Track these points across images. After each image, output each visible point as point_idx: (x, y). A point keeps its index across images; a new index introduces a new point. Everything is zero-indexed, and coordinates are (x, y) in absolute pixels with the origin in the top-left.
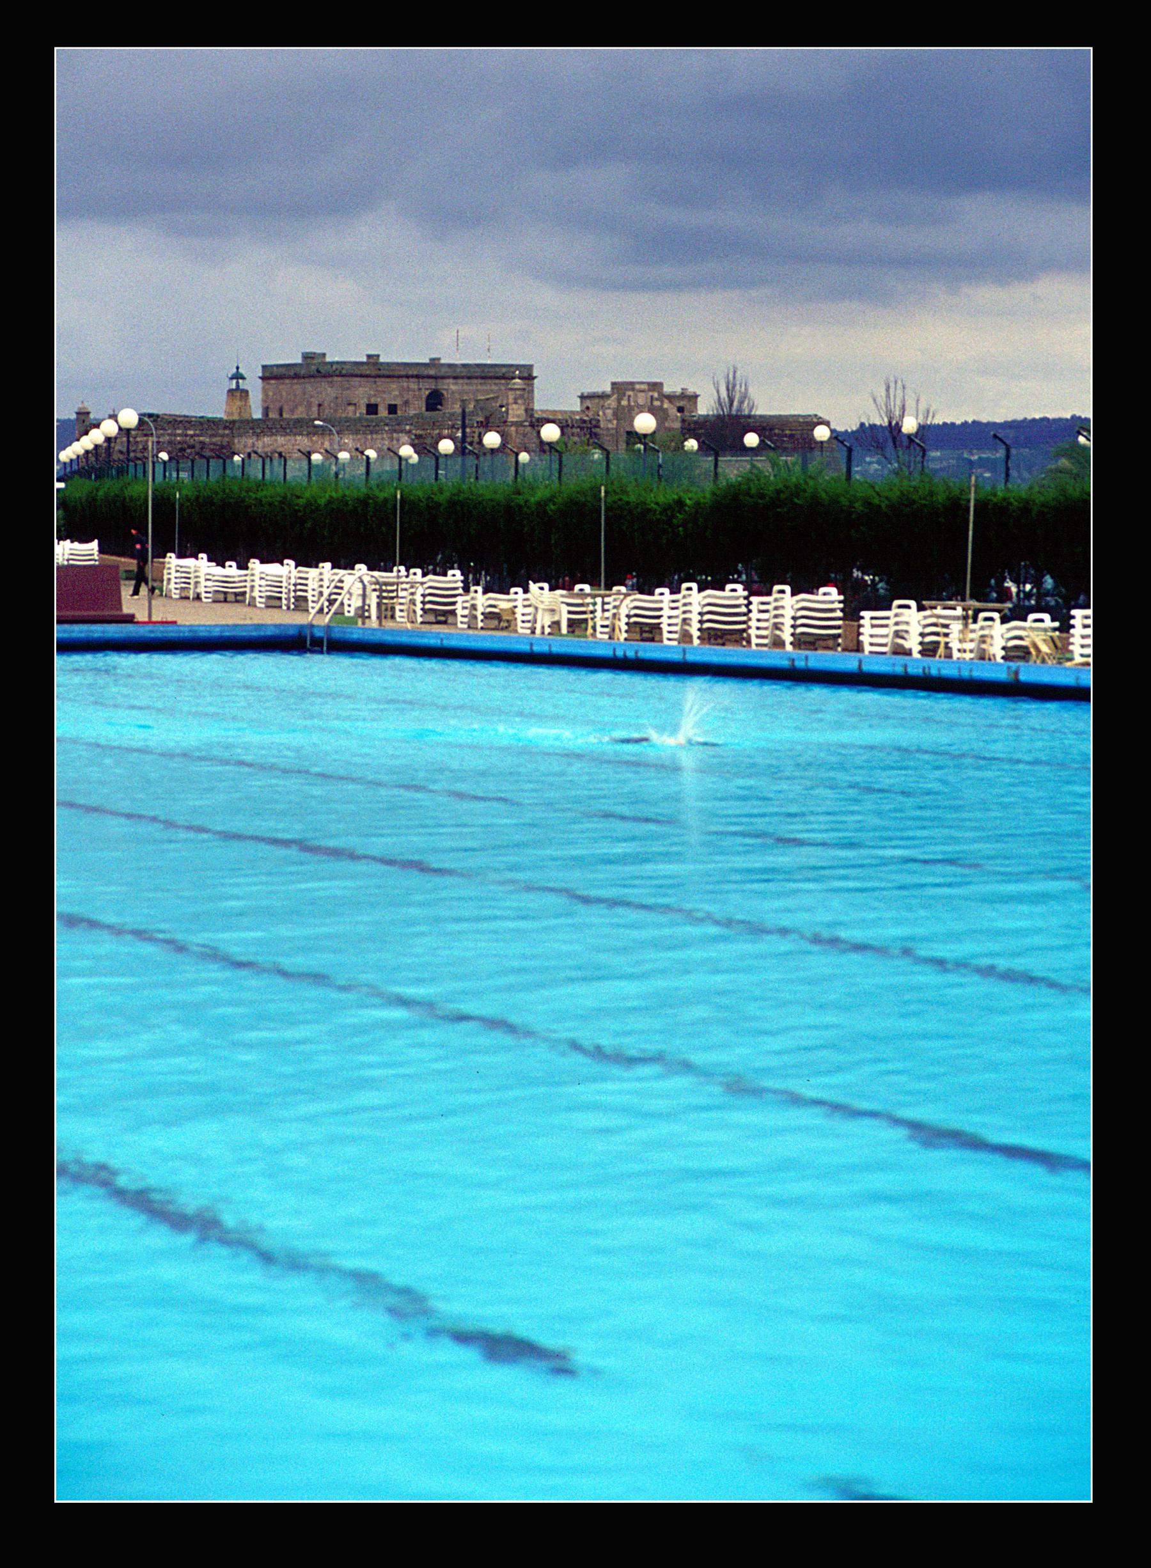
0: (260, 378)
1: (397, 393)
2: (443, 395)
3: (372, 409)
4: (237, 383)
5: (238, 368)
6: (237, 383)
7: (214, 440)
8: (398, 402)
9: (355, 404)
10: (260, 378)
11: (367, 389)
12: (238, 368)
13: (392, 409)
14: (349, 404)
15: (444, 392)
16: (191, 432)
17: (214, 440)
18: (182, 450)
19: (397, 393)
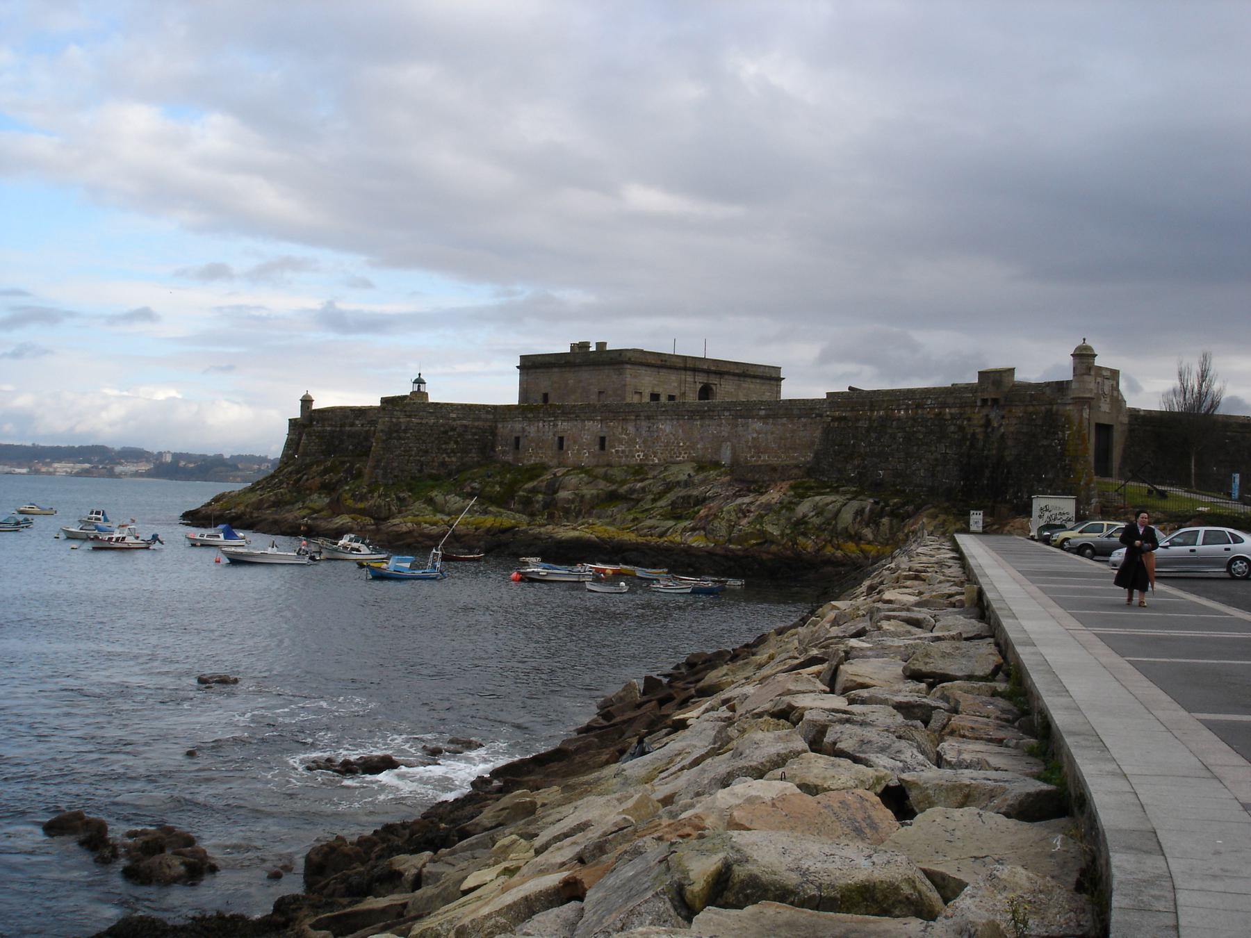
0: (517, 367)
1: (676, 384)
2: (712, 389)
3: (655, 397)
4: (419, 386)
5: (420, 374)
6: (419, 386)
7: (476, 424)
8: (676, 393)
9: (641, 393)
10: (517, 367)
11: (652, 379)
12: (420, 374)
13: (671, 398)
14: (636, 393)
15: (714, 387)
16: (454, 416)
17: (476, 424)
18: (446, 432)
19: (676, 384)
